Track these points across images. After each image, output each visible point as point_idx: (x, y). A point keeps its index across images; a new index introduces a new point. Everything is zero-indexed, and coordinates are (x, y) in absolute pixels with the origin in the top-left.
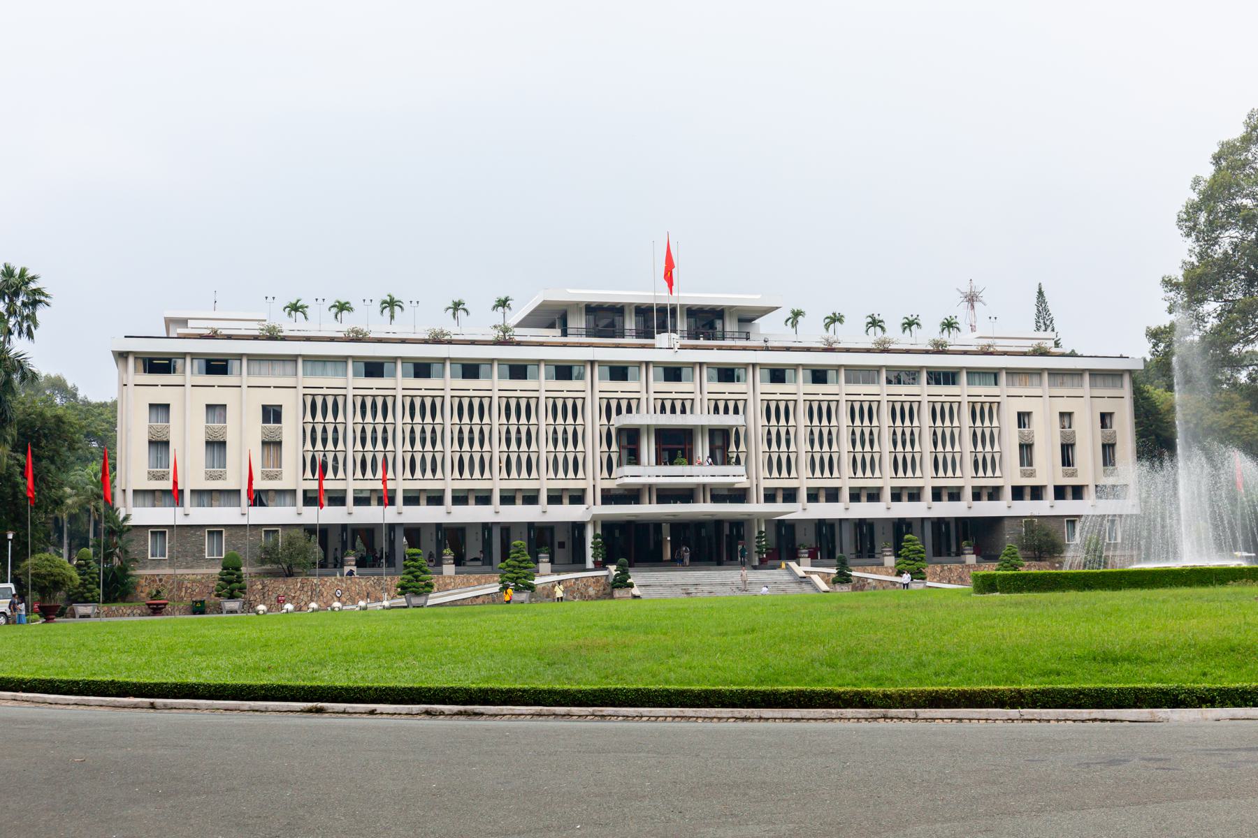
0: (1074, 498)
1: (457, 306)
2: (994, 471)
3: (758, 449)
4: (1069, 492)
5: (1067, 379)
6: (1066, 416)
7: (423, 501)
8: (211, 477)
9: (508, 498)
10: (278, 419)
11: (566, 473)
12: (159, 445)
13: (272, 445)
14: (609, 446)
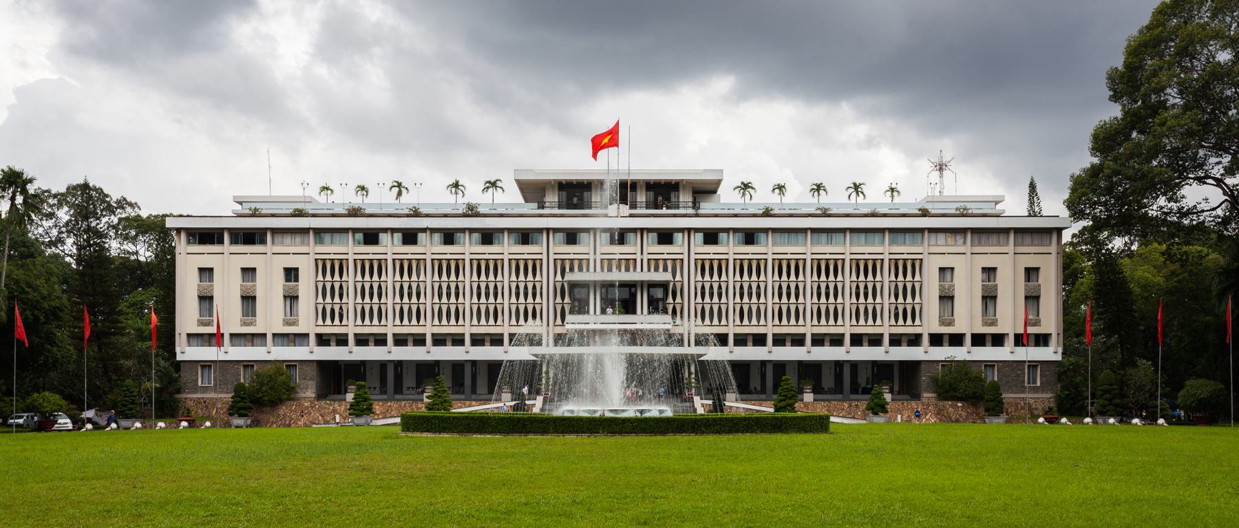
0: (993, 345)
1: (456, 185)
2: (913, 320)
3: (691, 301)
4: (989, 339)
5: (994, 238)
6: (990, 272)
7: (411, 343)
8: (244, 324)
9: (857, 340)
10: (297, 280)
11: (866, 321)
12: (206, 299)
13: (291, 298)
14: (563, 298)
